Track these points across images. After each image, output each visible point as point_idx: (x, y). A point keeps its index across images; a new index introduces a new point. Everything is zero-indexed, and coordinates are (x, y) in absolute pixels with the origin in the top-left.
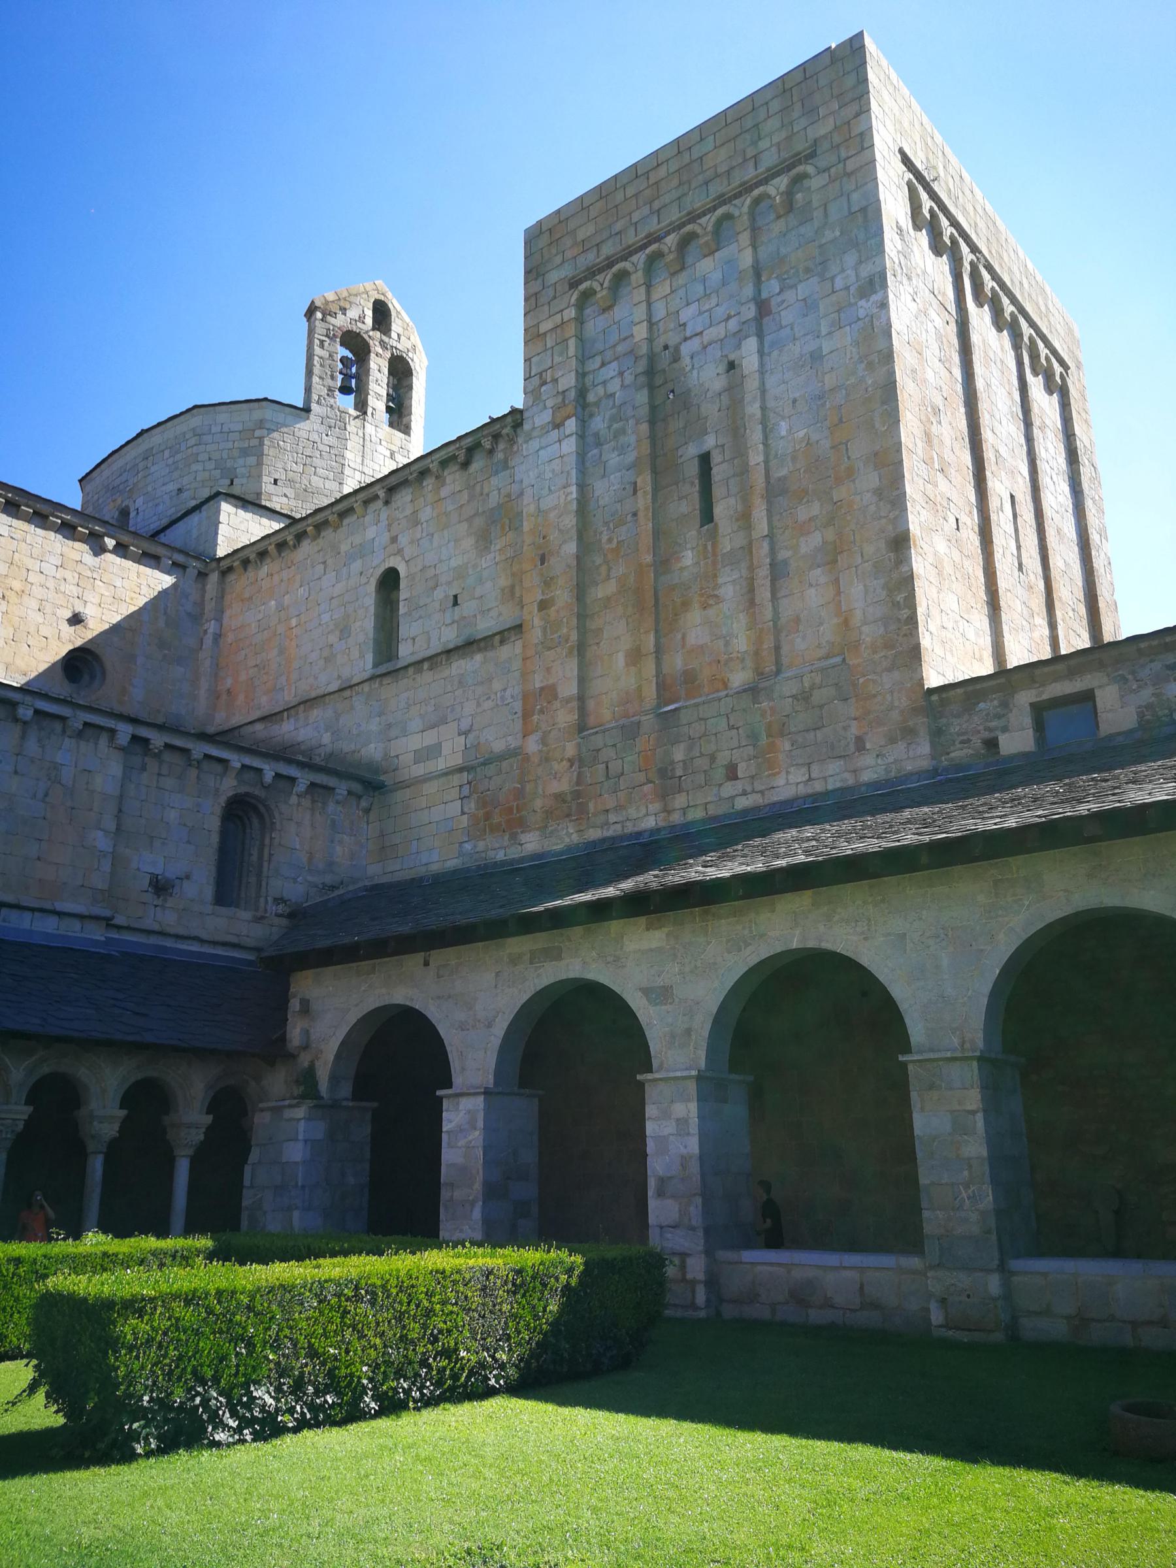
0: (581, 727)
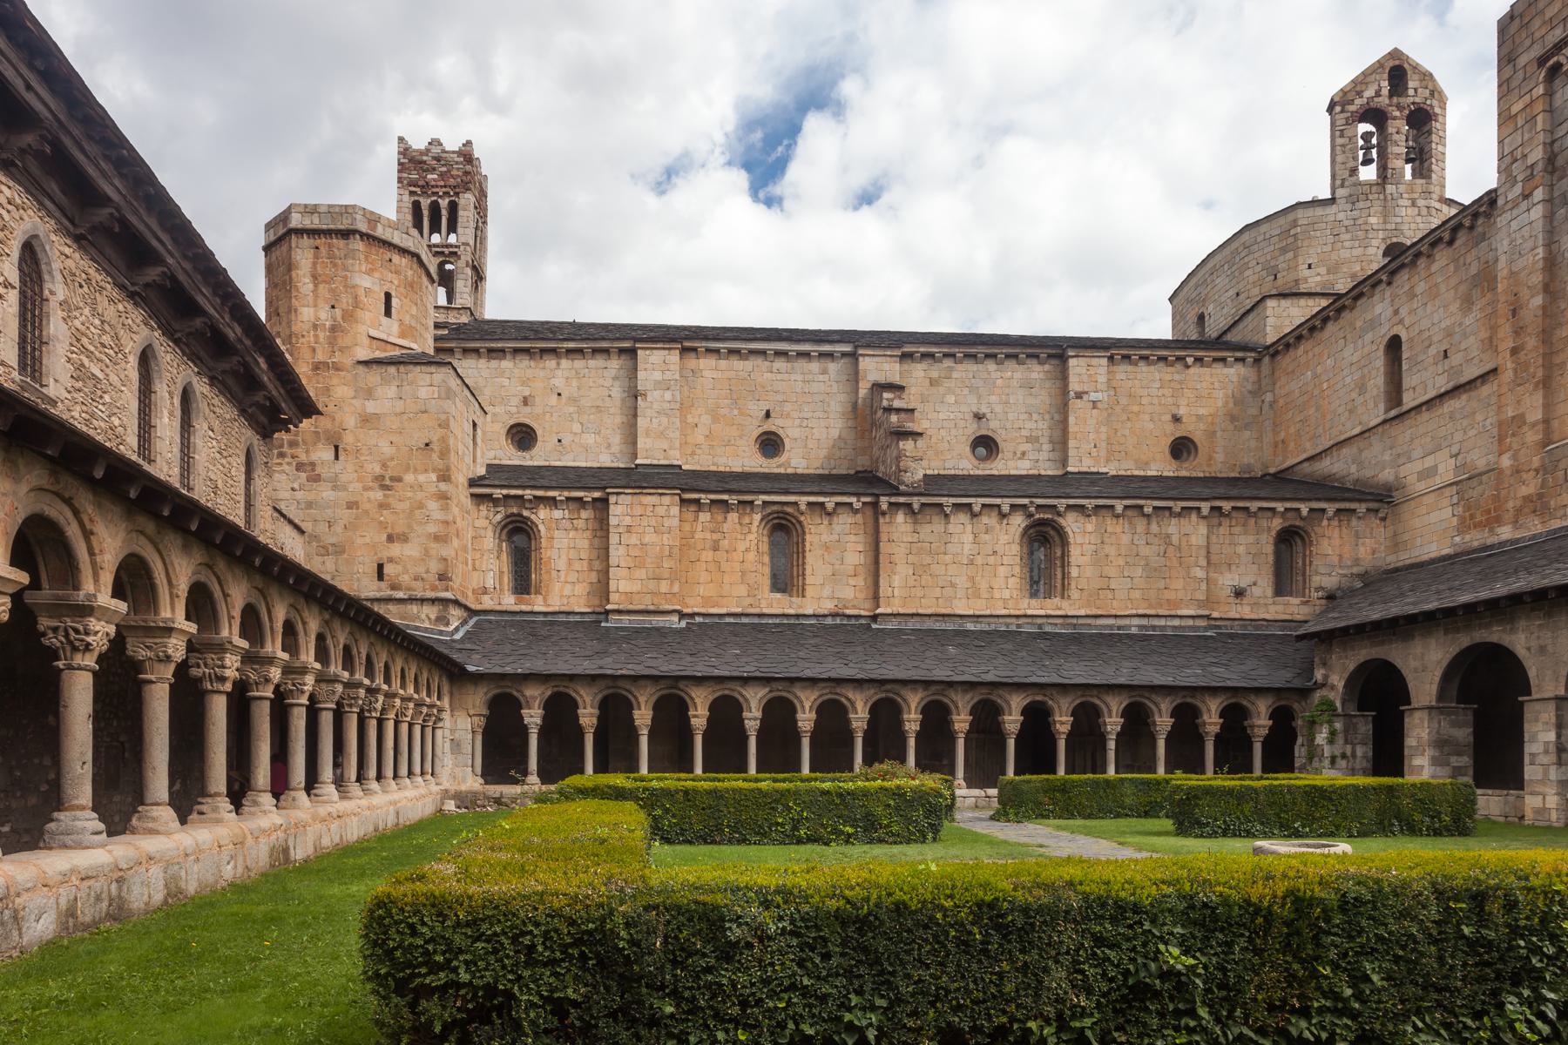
0: (1546, 442)
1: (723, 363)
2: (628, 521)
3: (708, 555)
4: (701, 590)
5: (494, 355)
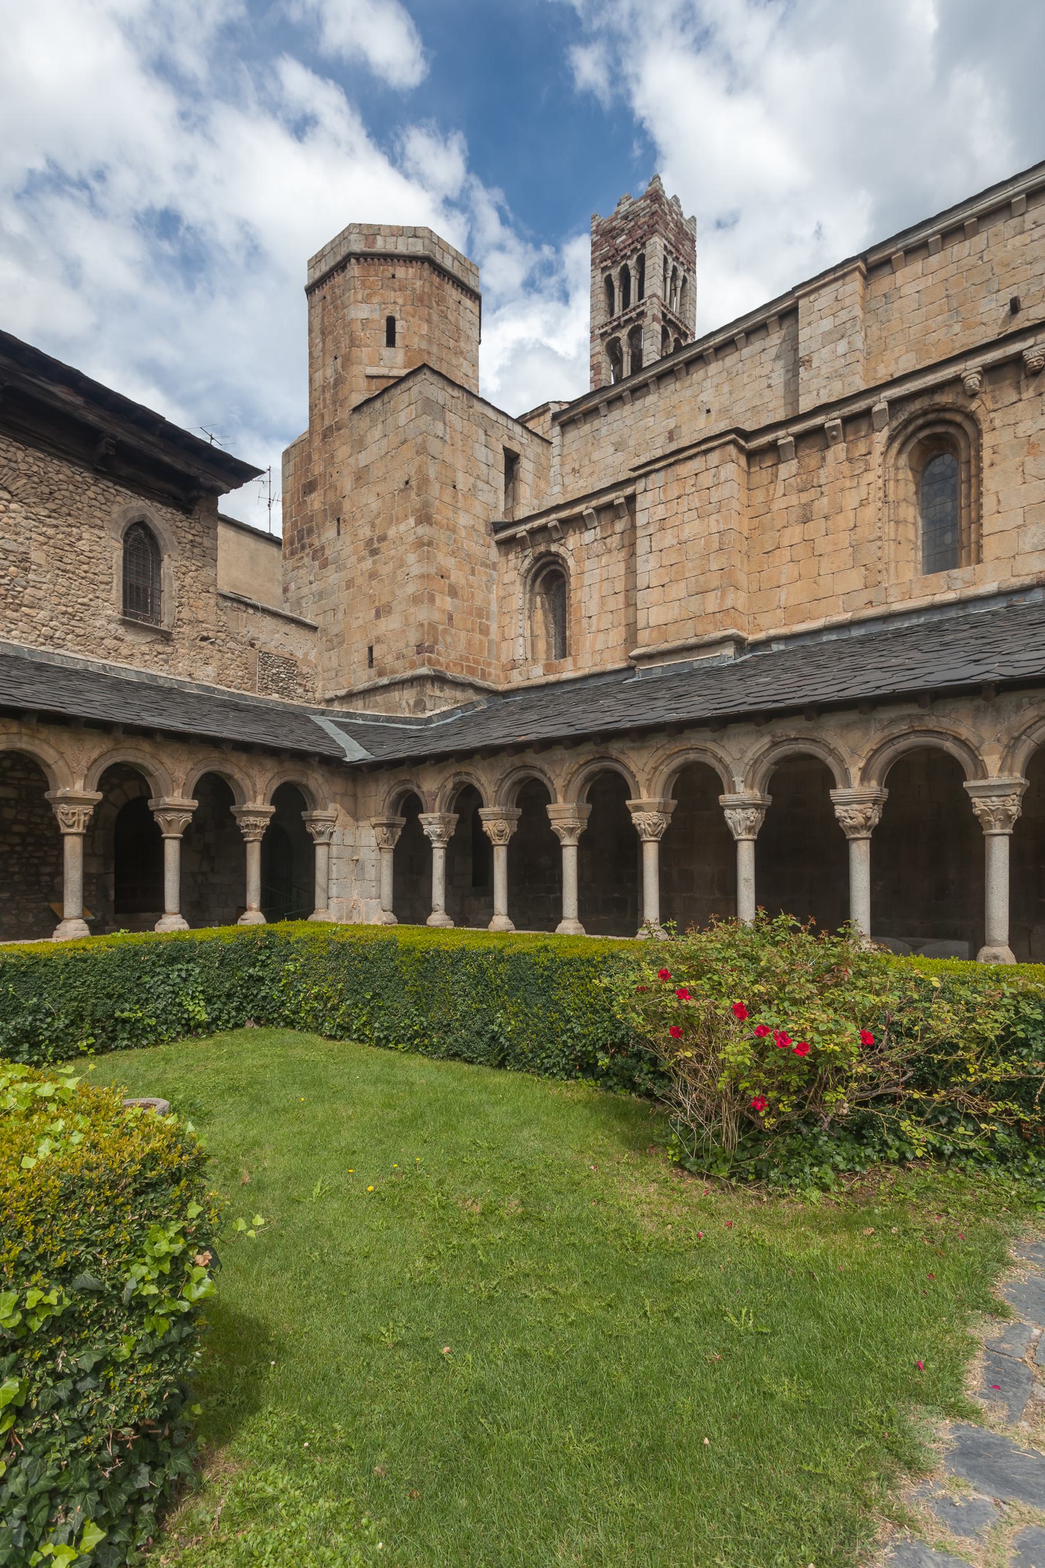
1: (935, 260)
2: (660, 512)
3: (795, 533)
4: (783, 597)
5: (638, 394)
